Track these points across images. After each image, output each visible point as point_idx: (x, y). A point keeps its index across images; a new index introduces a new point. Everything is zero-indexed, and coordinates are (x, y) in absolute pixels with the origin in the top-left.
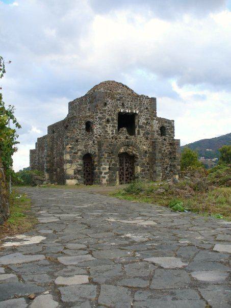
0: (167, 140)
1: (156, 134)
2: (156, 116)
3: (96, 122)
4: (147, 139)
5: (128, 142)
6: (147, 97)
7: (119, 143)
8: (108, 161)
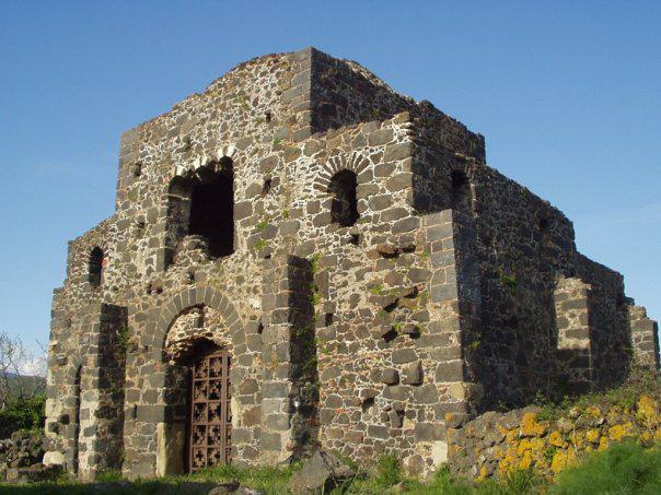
0: (368, 236)
1: (305, 222)
5: (193, 292)
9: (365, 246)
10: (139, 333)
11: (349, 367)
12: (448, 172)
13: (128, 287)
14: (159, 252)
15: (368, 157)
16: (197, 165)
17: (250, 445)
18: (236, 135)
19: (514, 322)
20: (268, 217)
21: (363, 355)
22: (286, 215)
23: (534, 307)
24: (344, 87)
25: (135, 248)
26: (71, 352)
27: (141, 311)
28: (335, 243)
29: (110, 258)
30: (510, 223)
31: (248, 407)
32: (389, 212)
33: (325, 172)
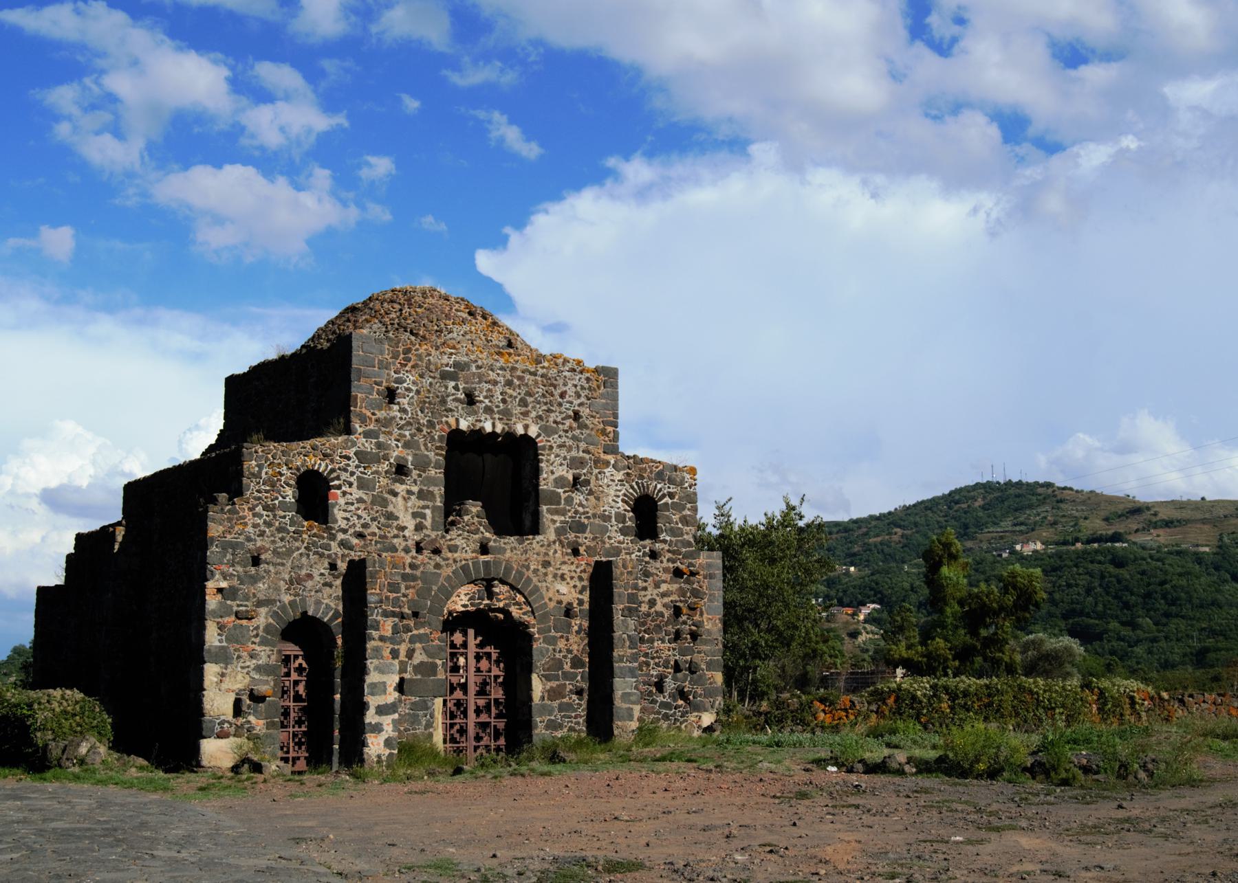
1: (614, 526)
2: (612, 449)
3: (344, 476)
4: (576, 552)
5: (486, 563)
6: (579, 363)
7: (447, 571)
8: (395, 653)
11: (646, 655)
14: (434, 509)
20: (576, 512)
22: (594, 516)
28: (638, 554)
29: (344, 493)
33: (631, 491)
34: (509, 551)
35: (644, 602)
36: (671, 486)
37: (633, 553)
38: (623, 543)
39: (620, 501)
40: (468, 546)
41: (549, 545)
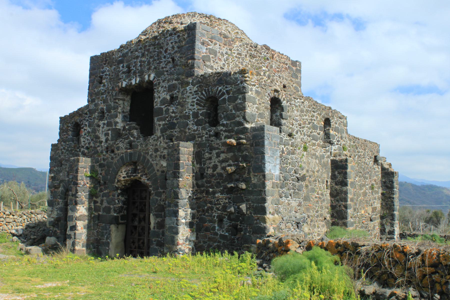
2: (191, 74)
5: (131, 154)
7: (115, 160)
9: (221, 139)
10: (101, 174)
11: (211, 202)
12: (268, 99)
13: (95, 148)
15: (225, 91)
16: (133, 82)
17: (160, 239)
18: (155, 68)
19: (303, 178)
20: (171, 117)
21: (218, 197)
22: (180, 117)
23: (317, 168)
24: (215, 44)
25: (99, 126)
26: (62, 181)
27: (102, 162)
28: (206, 136)
29: (85, 130)
30: (305, 123)
31: (159, 220)
32: (234, 123)
33: (202, 96)
34: (139, 146)
35: (209, 167)
36: (228, 86)
37: (203, 136)
38: (196, 131)
39: (195, 105)
40: (123, 146)
41: (158, 139)
